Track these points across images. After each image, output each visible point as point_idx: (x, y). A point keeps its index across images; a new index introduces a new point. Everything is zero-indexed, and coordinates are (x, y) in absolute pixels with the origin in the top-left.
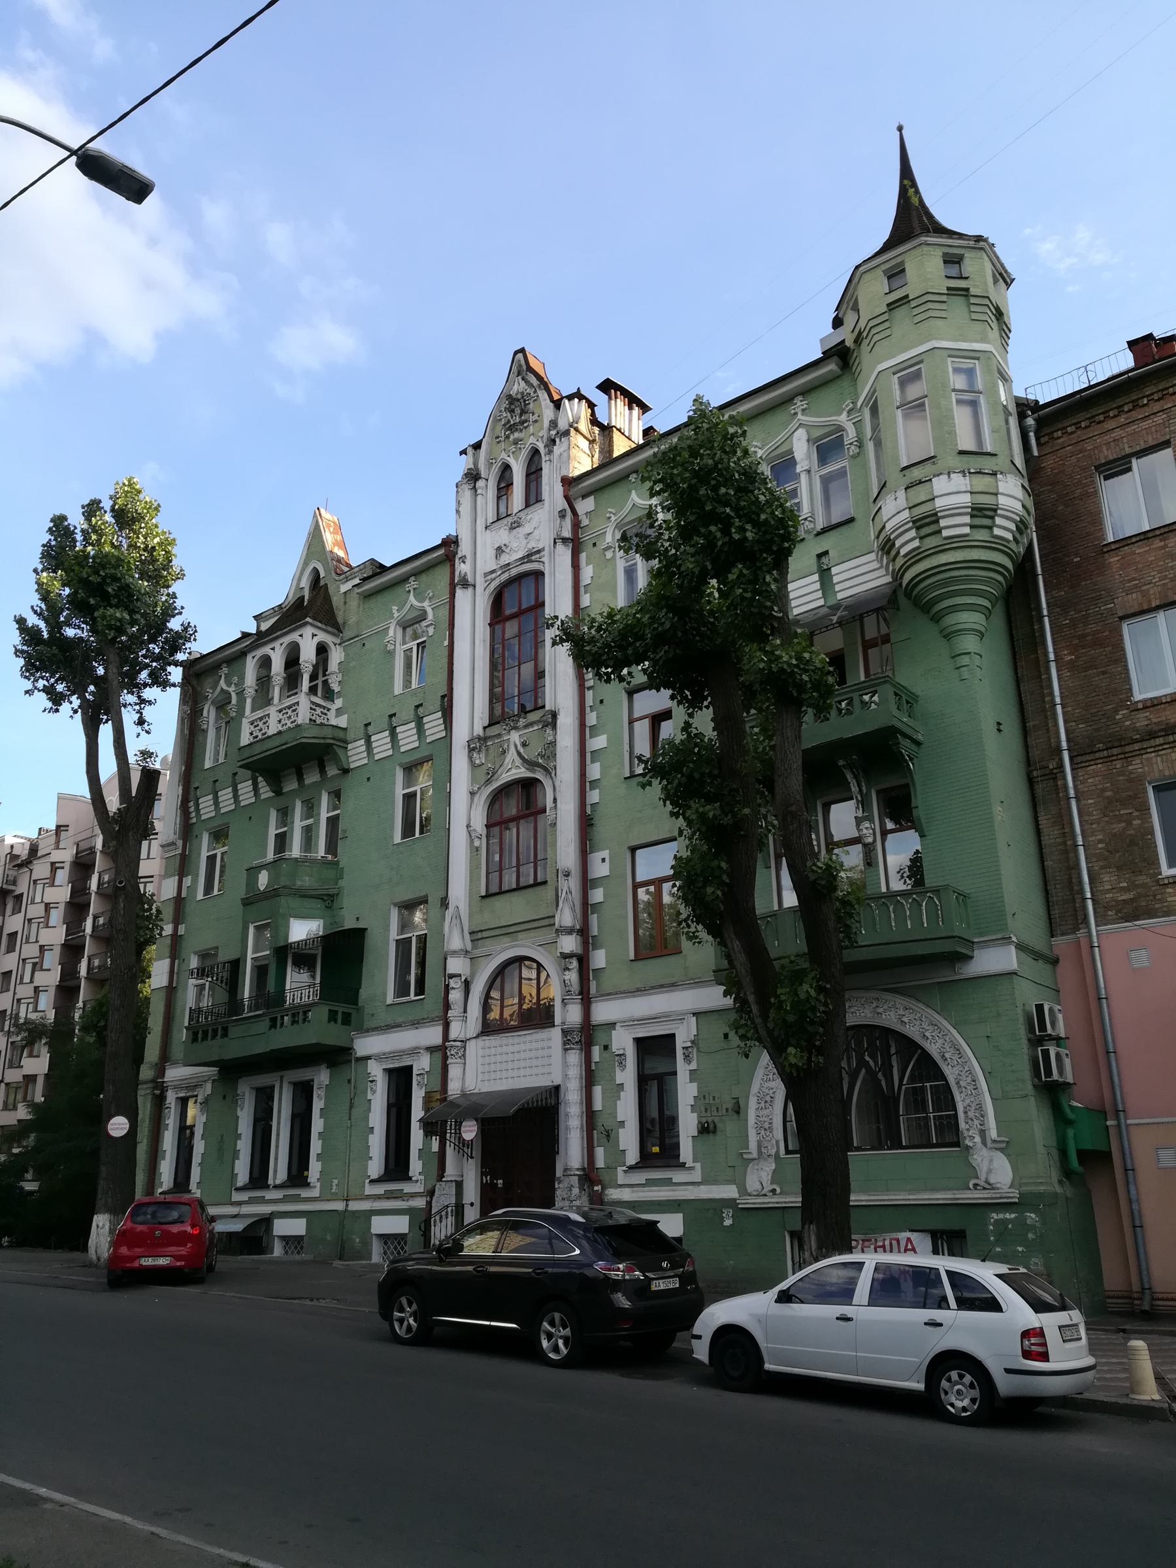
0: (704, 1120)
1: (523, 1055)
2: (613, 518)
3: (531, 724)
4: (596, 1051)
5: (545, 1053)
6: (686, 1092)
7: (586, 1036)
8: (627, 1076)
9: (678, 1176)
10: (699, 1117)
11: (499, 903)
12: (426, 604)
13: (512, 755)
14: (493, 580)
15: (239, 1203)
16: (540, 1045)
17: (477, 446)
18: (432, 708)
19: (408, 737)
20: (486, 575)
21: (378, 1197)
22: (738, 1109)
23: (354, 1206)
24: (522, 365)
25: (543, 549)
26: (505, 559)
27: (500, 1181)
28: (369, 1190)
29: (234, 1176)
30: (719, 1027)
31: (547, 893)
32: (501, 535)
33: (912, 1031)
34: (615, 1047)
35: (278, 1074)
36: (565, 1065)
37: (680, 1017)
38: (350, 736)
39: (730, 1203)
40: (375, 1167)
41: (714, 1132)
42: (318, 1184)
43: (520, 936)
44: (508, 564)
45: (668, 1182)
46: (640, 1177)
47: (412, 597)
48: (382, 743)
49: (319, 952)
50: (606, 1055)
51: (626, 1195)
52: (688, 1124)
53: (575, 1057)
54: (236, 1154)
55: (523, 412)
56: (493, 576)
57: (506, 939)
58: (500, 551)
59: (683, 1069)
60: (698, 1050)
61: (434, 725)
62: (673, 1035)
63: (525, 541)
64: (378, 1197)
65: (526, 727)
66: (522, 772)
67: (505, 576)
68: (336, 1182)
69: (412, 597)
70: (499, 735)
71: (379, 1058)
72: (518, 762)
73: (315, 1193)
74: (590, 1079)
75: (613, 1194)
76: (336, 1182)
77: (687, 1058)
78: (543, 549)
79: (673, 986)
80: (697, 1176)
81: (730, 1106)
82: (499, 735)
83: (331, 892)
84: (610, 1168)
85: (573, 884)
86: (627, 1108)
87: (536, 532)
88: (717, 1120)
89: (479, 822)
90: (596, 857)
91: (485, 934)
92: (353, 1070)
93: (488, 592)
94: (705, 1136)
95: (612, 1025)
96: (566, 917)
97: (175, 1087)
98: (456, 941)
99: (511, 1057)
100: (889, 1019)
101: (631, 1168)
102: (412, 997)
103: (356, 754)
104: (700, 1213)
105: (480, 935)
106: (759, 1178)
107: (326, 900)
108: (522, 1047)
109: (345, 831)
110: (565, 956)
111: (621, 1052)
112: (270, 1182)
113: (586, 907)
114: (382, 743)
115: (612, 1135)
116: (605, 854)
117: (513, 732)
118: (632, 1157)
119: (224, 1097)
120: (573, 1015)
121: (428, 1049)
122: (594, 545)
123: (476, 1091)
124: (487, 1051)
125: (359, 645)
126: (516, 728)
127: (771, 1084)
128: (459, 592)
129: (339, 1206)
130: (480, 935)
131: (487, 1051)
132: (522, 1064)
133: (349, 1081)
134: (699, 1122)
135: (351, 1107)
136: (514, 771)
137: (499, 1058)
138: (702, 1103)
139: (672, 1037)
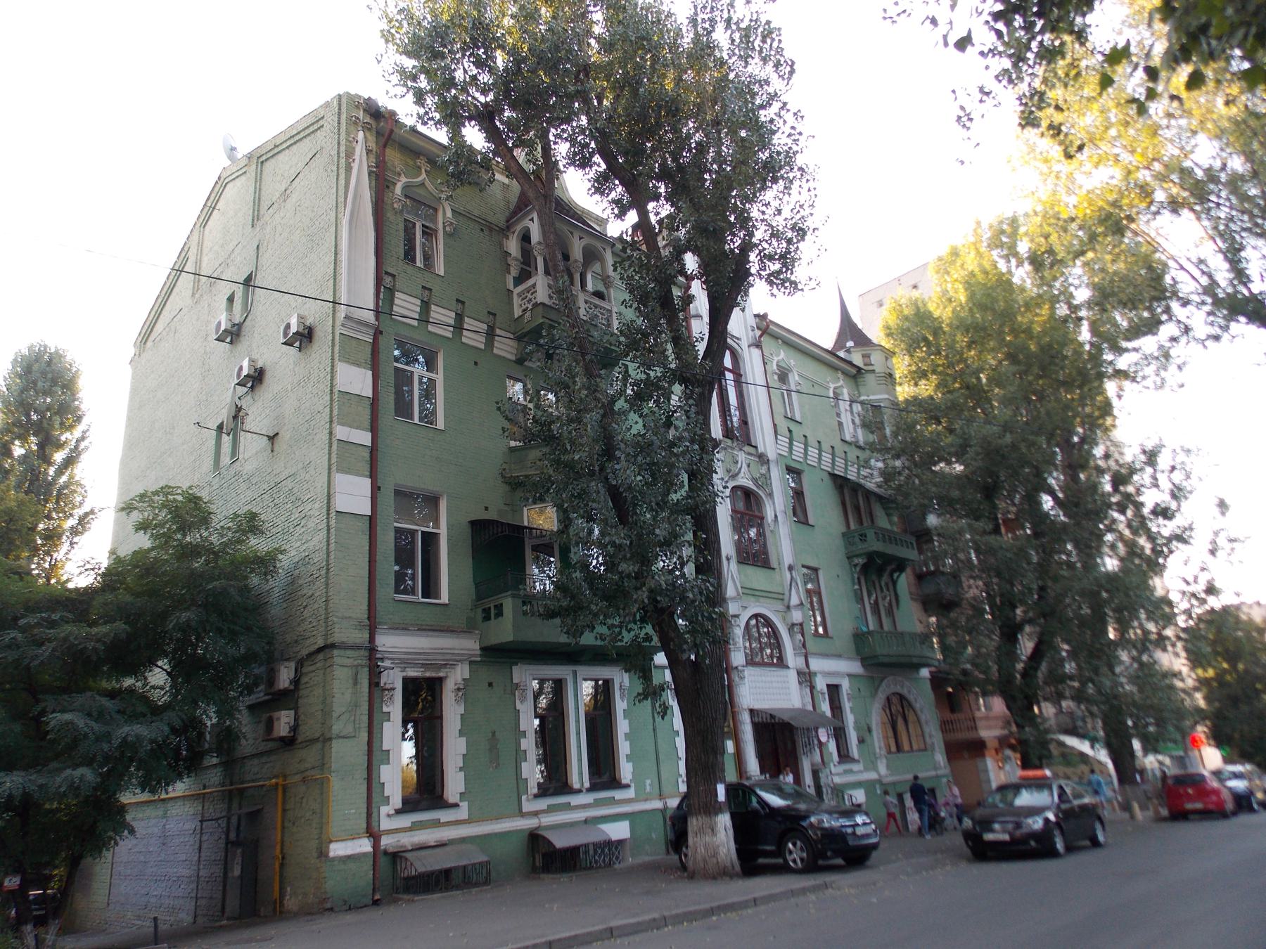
2: (776, 359)
6: (850, 719)
7: (806, 678)
9: (855, 767)
15: (536, 814)
22: (870, 730)
29: (520, 783)
31: (776, 575)
33: (911, 698)
35: (570, 668)
36: (802, 697)
39: (879, 781)
54: (520, 756)
57: (752, 599)
65: (749, 454)
66: (750, 484)
68: (648, 782)
76: (648, 782)
97: (404, 663)
100: (905, 692)
104: (868, 786)
106: (883, 769)
110: (793, 625)
112: (576, 786)
119: (490, 685)
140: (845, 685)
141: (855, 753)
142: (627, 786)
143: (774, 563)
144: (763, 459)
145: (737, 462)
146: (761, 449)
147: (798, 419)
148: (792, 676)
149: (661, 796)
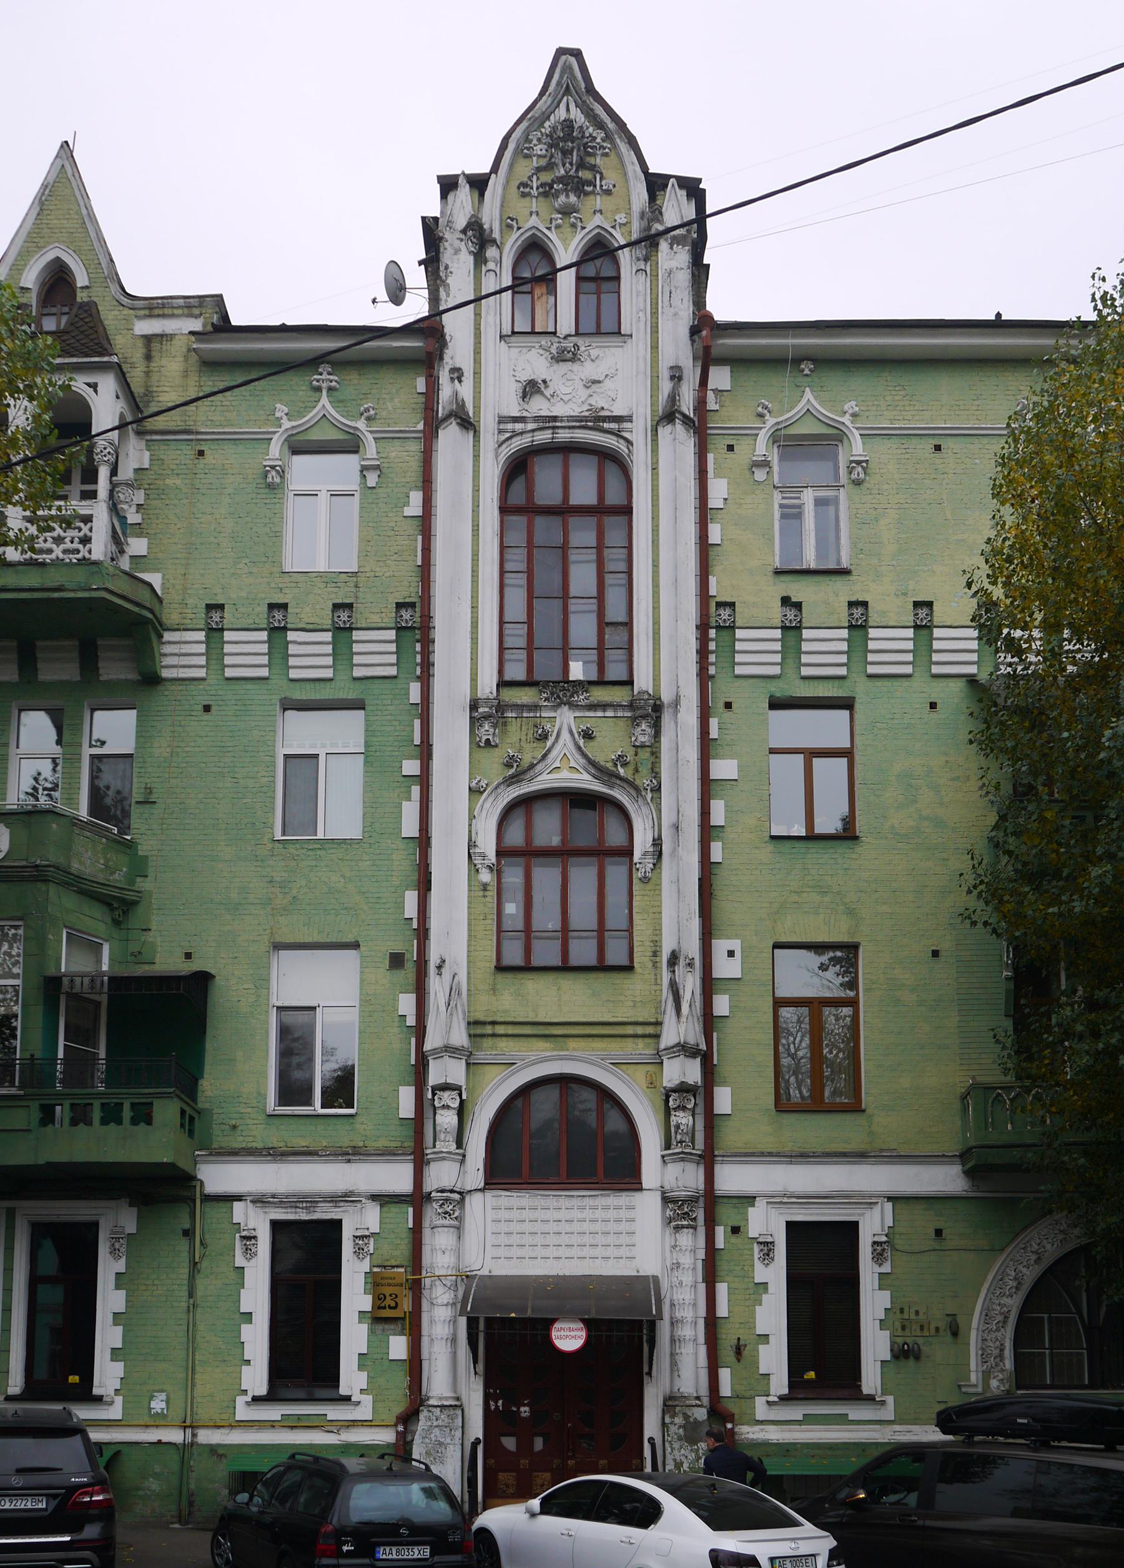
0: (900, 1340)
1: (576, 1227)
2: (771, 421)
3: (604, 706)
4: (720, 1232)
5: (623, 1227)
6: (873, 1303)
7: (703, 1211)
8: (774, 1275)
10: (893, 1336)
11: (533, 985)
12: (361, 424)
13: (564, 747)
14: (515, 434)
16: (611, 1214)
17: (479, 183)
18: (375, 619)
19: (311, 655)
20: (502, 420)
21: (272, 1425)
23: (206, 1437)
24: (569, 73)
25: (629, 419)
26: (539, 406)
27: (525, 1411)
28: (243, 1412)
30: (925, 1221)
31: (635, 986)
32: (534, 362)
34: (753, 1233)
37: (867, 1201)
38: (171, 616)
40: (256, 1377)
41: (917, 1358)
42: (119, 1400)
43: (572, 1043)
44: (555, 418)
45: (842, 1419)
46: (796, 1412)
47: (324, 400)
48: (246, 651)
49: (104, 999)
50: (734, 1239)
51: (774, 1434)
52: (875, 1345)
53: (691, 1243)
55: (581, 165)
56: (519, 427)
57: (541, 1044)
58: (531, 389)
59: (868, 1272)
60: (894, 1249)
61: (376, 652)
62: (854, 1225)
63: (583, 393)
64: (272, 1425)
65: (592, 707)
66: (585, 781)
67: (544, 437)
69: (324, 400)
70: (535, 707)
71: (260, 1201)
72: (576, 760)
73: (115, 1412)
74: (711, 1277)
75: (749, 1433)
77: (878, 1257)
78: (629, 419)
79: (860, 1156)
80: (888, 1413)
81: (942, 1325)
82: (535, 707)
83: (130, 896)
84: (744, 1397)
85: (691, 984)
86: (772, 1316)
87: (608, 383)
88: (920, 1341)
89: (488, 845)
90: (720, 946)
91: (500, 1030)
92: (208, 1218)
93: (506, 451)
94: (903, 1362)
95: (750, 1200)
96: (679, 1029)
98: (446, 1028)
99: (554, 1227)
101: (782, 1398)
102: (317, 1107)
103: (182, 653)
105: (489, 1030)
107: (121, 907)
108: (579, 1215)
109: (149, 790)
111: (770, 1239)
113: (709, 1021)
114: (246, 651)
115: (746, 1353)
116: (735, 944)
117: (565, 709)
118: (780, 1384)
120: (687, 1178)
121: (374, 1197)
122: (731, 448)
123: (485, 1272)
124: (505, 1215)
125: (189, 451)
126: (573, 706)
127: (1004, 1300)
128: (450, 437)
129: (175, 1436)
130: (489, 1030)
131: (505, 1215)
132: (576, 1240)
133: (188, 1233)
134: (892, 1344)
135: (192, 1278)
136: (565, 774)
137: (527, 1227)
138: (897, 1318)
139: (852, 1228)
140: (872, 1226)
141: (871, 1379)
142: (99, 1399)
143: (641, 958)
144: (651, 712)
145: (544, 737)
146: (643, 681)
147: (845, 564)
148: (645, 1209)
149: (189, 1425)
